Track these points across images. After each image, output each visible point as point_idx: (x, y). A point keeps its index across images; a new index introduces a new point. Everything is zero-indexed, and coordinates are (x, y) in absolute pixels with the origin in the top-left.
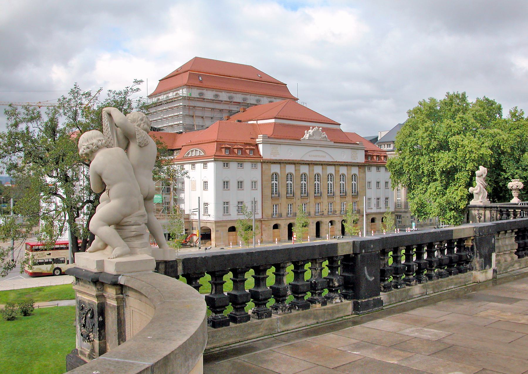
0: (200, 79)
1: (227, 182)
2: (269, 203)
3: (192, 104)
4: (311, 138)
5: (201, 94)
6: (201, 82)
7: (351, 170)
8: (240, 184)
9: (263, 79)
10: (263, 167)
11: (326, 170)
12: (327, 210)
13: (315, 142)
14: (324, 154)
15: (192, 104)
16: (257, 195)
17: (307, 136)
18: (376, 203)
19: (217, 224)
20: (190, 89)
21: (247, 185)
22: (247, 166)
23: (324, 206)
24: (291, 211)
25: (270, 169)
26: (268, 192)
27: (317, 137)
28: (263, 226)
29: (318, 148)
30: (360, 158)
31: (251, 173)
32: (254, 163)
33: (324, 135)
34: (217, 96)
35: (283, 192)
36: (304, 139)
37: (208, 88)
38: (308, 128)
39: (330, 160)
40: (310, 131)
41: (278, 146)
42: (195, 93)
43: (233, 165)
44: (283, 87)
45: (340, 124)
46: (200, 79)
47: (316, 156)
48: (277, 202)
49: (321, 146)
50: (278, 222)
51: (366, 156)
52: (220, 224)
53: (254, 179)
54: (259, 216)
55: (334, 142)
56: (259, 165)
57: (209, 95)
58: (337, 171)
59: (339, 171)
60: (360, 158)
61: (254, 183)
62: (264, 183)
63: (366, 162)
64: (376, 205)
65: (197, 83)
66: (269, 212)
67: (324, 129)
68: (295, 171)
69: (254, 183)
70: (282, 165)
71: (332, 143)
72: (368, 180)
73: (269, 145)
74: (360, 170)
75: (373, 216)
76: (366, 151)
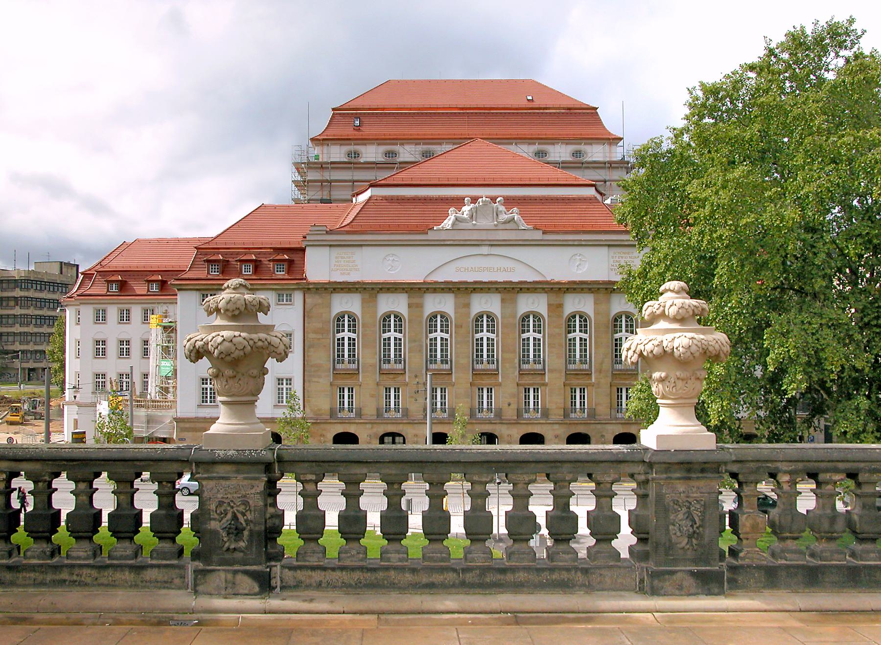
2: (323, 382)
3: (326, 175)
5: (390, 154)
6: (358, 129)
7: (609, 301)
12: (514, 406)
13: (475, 236)
14: (508, 264)
15: (326, 175)
17: (448, 223)
19: (182, 425)
20: (325, 147)
23: (504, 395)
25: (329, 306)
26: (323, 358)
29: (485, 250)
33: (515, 213)
34: (357, 154)
35: (367, 357)
37: (365, 141)
38: (458, 202)
39: (530, 277)
40: (464, 209)
42: (337, 153)
44: (590, 114)
50: (352, 429)
52: (187, 425)
55: (544, 233)
56: (298, 297)
57: (371, 153)
58: (556, 308)
59: (560, 306)
62: (311, 336)
65: (349, 131)
66: (323, 404)
67: (509, 202)
68: (410, 306)
71: (538, 235)
73: (605, 250)
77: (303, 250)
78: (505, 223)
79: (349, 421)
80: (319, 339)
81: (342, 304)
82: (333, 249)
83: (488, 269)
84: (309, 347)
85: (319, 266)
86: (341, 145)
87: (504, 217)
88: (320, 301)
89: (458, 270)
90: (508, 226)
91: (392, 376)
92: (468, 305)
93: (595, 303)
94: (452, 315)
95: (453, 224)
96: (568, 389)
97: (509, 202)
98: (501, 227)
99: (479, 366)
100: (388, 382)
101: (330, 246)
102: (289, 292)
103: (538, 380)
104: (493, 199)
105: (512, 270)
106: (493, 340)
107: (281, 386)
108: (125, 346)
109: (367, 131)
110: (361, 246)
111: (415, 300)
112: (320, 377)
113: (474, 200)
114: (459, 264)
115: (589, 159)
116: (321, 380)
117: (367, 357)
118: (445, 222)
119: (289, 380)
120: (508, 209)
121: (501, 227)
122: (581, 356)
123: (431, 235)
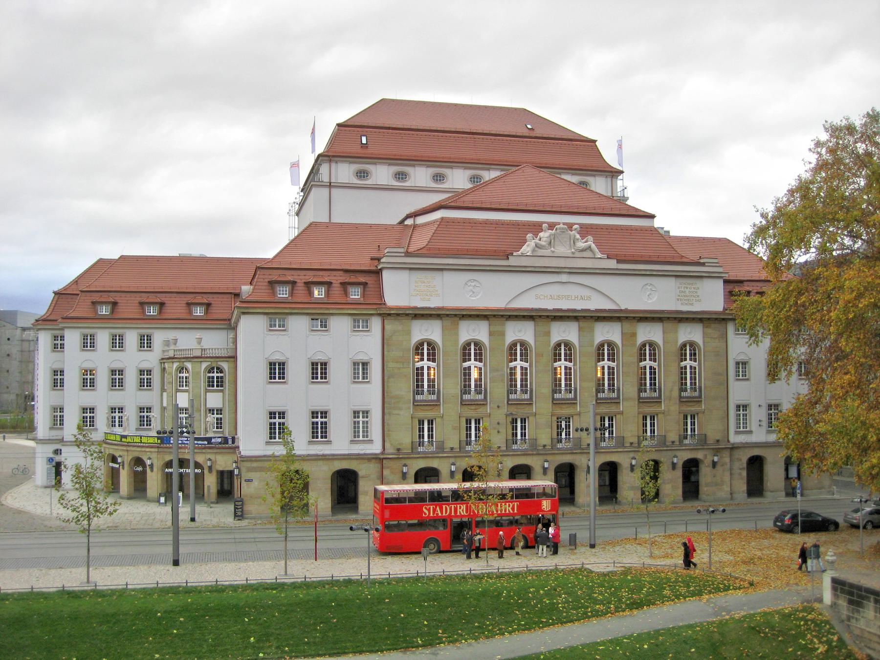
0: (364, 140)
1: (745, 363)
4: (540, 252)
6: (364, 146)
7: (676, 332)
8: (319, 370)
9: (538, 132)
10: (387, 327)
11: (592, 331)
14: (586, 292)
16: (370, 395)
17: (527, 249)
18: (765, 419)
21: (340, 371)
22: (340, 325)
24: (693, 430)
25: (409, 333)
26: (403, 388)
27: (561, 249)
28: (386, 472)
29: (564, 278)
30: (711, 297)
31: (349, 342)
32: (359, 318)
33: (590, 242)
36: (522, 255)
38: (536, 228)
40: (541, 234)
41: (437, 275)
43: (299, 325)
45: (652, 217)
46: (364, 140)
47: (559, 297)
48: (693, 409)
49: (572, 272)
50: (434, 464)
51: (730, 295)
52: (255, 464)
53: (362, 357)
54: (376, 448)
55: (619, 262)
56: (376, 324)
59: (634, 335)
60: (711, 297)
61: (361, 368)
62: (390, 365)
63: (725, 309)
64: (765, 423)
65: (355, 149)
66: (404, 438)
67: (585, 230)
68: (491, 334)
69: (361, 368)
70: (584, 324)
71: (612, 264)
72: (734, 354)
74: (709, 331)
75: (756, 452)
76: (726, 282)
77: (378, 273)
78: (583, 250)
79: (525, 454)
80: (399, 368)
81: (422, 331)
82: (413, 272)
83: (568, 297)
84: (389, 378)
85: (398, 290)
86: (350, 163)
87: (581, 244)
88: (400, 328)
89: (537, 297)
90: (585, 254)
91: (473, 407)
92: (548, 334)
93: (664, 333)
94: (660, 342)
95: (533, 251)
96: (555, 418)
97: (585, 230)
98: (578, 255)
99: (643, 395)
100: (470, 413)
101: (410, 269)
102: (365, 317)
103: (613, 409)
104: (570, 226)
105: (589, 298)
106: (570, 369)
107: (357, 420)
108: (89, 377)
109: (373, 150)
110: (442, 270)
111: (497, 328)
112: (400, 409)
113: (551, 226)
114: (539, 291)
115: (593, 188)
116: (401, 413)
117: (668, 382)
118: (524, 247)
119: (366, 413)
120: (583, 237)
121: (578, 255)
122: (691, 383)
123: (512, 261)
